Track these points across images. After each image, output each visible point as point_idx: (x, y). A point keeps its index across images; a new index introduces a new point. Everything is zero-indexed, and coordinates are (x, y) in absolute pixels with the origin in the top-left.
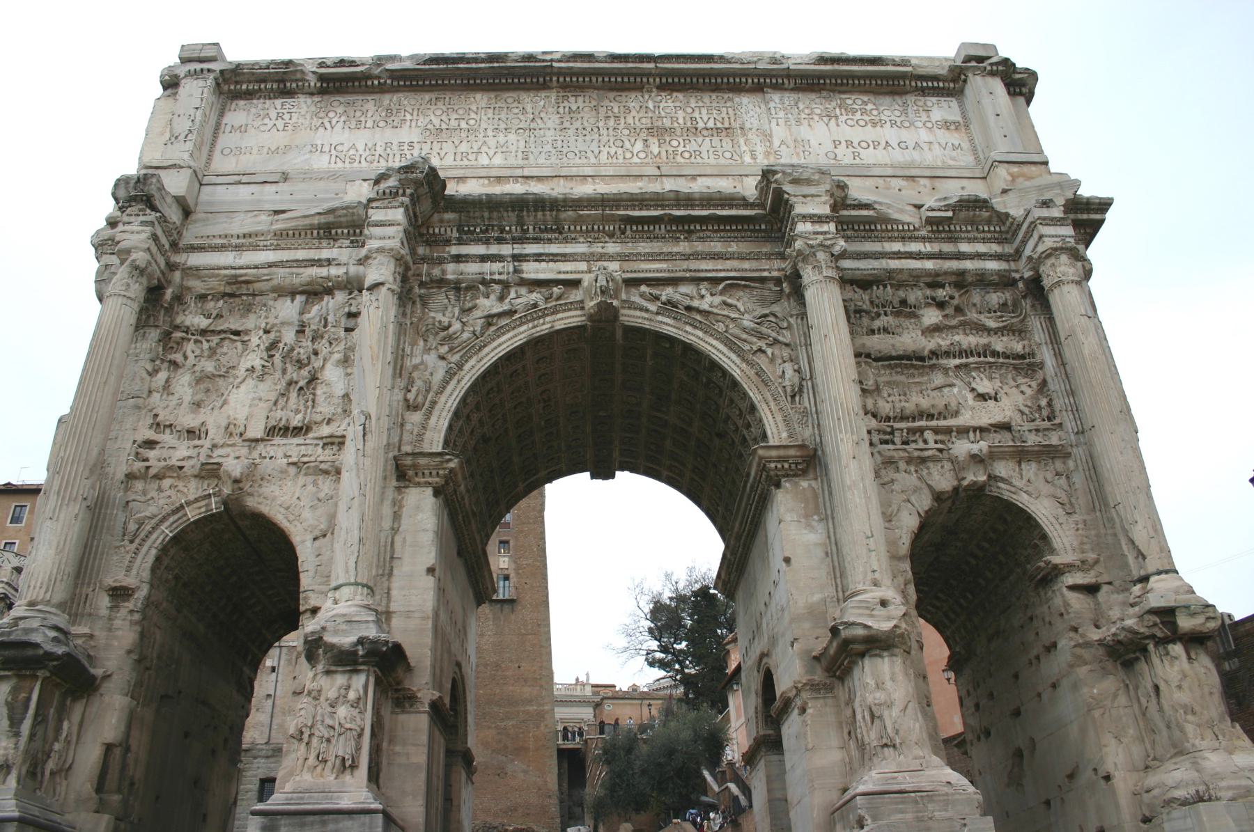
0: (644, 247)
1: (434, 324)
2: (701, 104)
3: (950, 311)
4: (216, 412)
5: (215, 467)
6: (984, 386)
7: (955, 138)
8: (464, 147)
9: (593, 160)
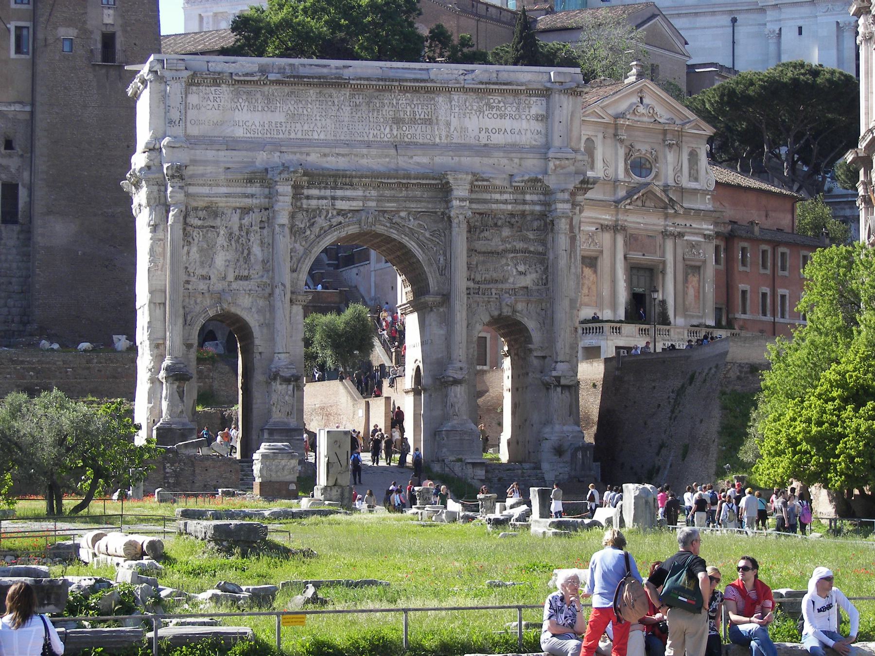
0: (387, 193)
2: (419, 102)
6: (521, 268)
7: (538, 126)
8: (306, 127)
9: (366, 138)
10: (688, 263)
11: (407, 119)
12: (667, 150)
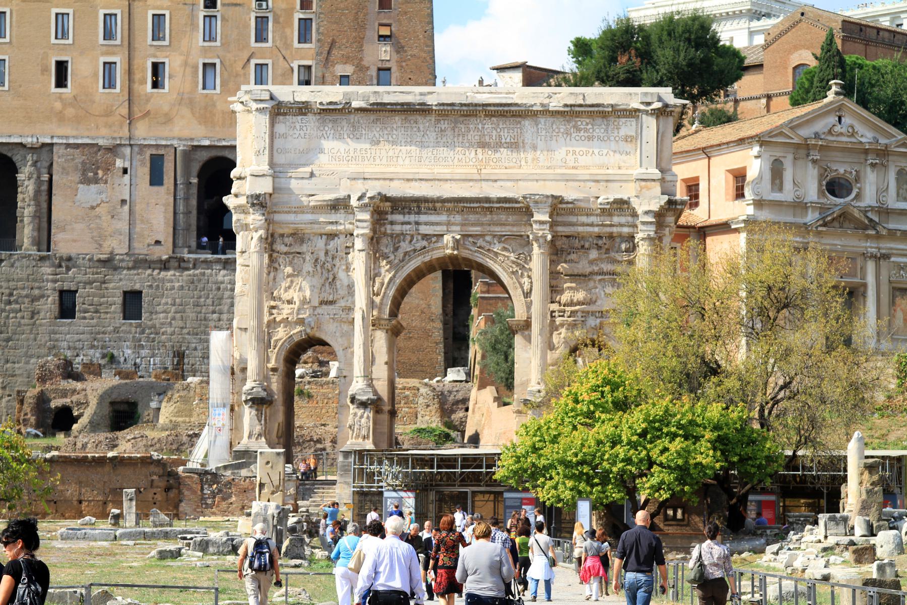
0: (472, 217)
3: (603, 251)
10: (894, 285)
12: (869, 169)
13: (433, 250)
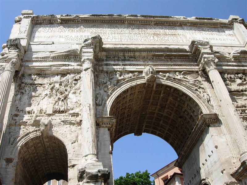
1: (101, 82)
2: (166, 28)
3: (243, 80)
4: (36, 106)
5: (38, 122)
7: (233, 38)
11: (162, 35)
13: (138, 78)
